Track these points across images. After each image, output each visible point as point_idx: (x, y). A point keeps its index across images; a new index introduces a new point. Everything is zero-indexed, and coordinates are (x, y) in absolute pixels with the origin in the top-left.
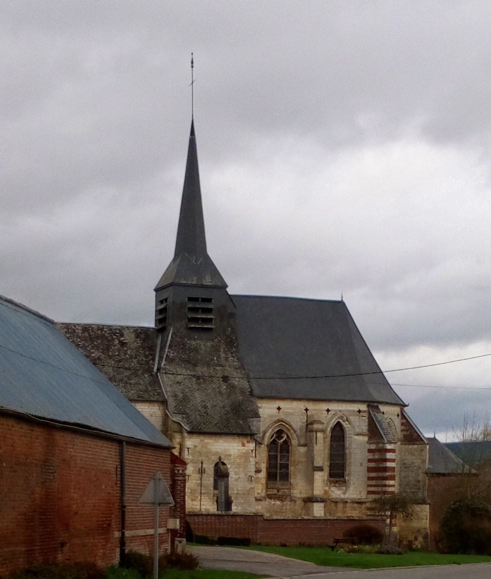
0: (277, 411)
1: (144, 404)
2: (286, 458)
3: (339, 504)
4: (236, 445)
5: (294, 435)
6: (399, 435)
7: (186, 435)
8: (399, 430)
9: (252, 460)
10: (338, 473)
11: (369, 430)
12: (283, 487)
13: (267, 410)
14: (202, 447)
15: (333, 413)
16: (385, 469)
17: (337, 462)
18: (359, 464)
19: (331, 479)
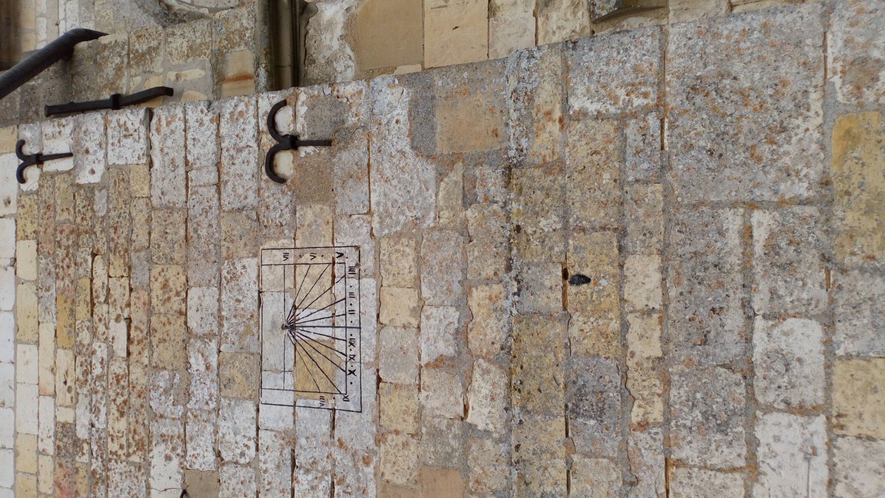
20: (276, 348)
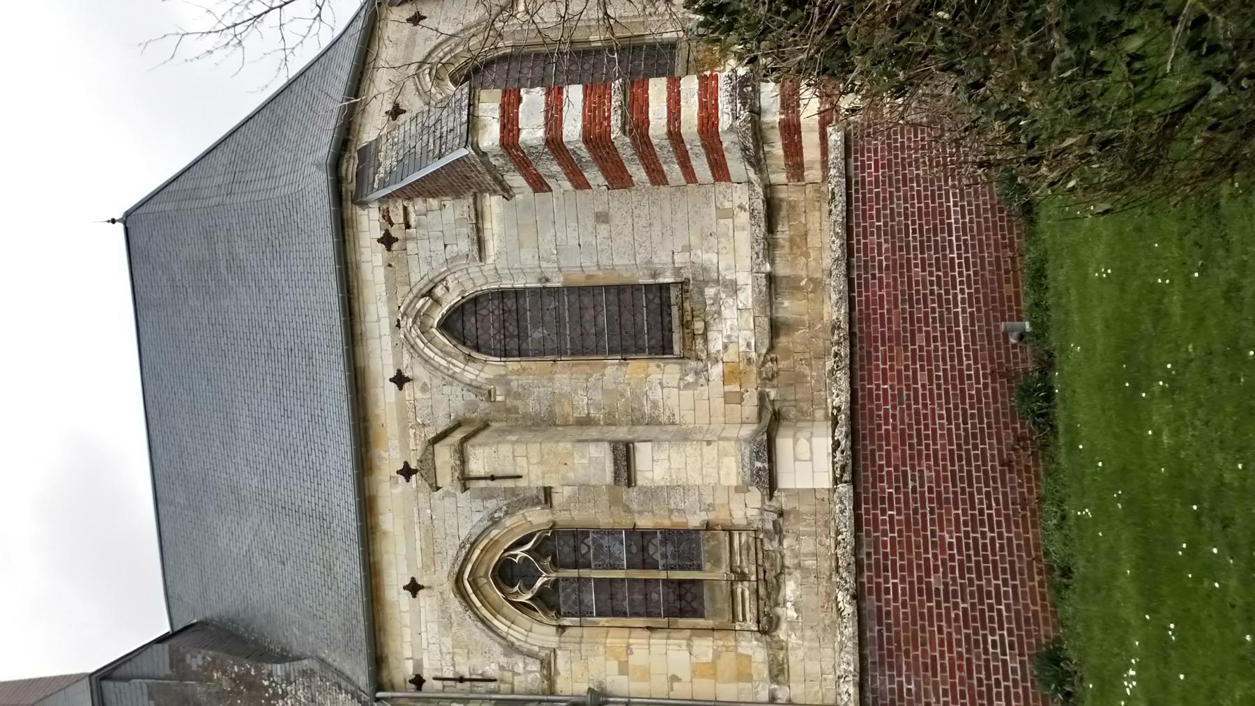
0: (421, 592)
2: (605, 542)
3: (781, 314)
5: (509, 522)
10: (651, 318)
11: (458, 195)
12: (725, 556)
15: (406, 358)
17: (603, 319)
18: (603, 229)
19: (677, 348)
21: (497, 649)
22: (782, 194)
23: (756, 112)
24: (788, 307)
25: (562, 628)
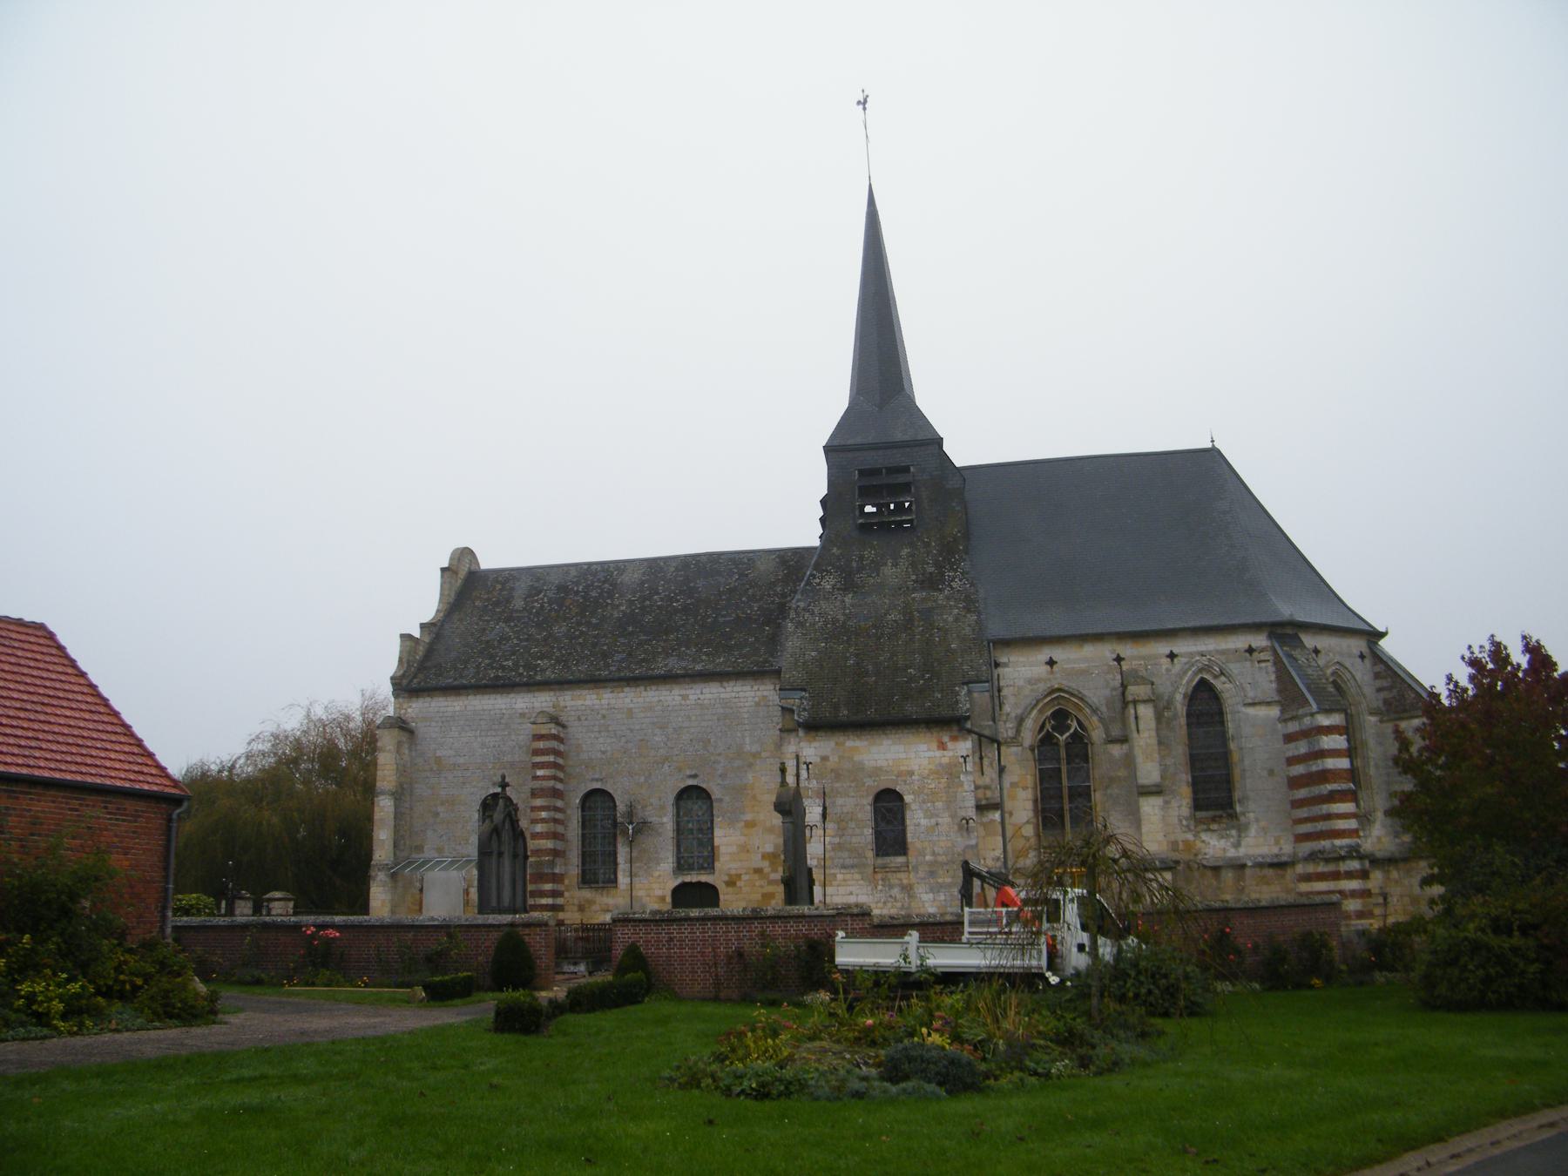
1: (740, 683)
3: (1224, 873)
4: (924, 747)
5: (1095, 719)
6: (1376, 700)
7: (801, 733)
8: (1369, 691)
9: (967, 782)
11: (1279, 691)
13: (1023, 672)
14: (840, 757)
15: (1184, 660)
16: (1324, 776)
17: (1210, 772)
18: (1265, 773)
19: (1199, 814)
20: (933, 821)
21: (1019, 711)
22: (1289, 871)
23: (1343, 858)
24: (1228, 876)
25: (1032, 749)
